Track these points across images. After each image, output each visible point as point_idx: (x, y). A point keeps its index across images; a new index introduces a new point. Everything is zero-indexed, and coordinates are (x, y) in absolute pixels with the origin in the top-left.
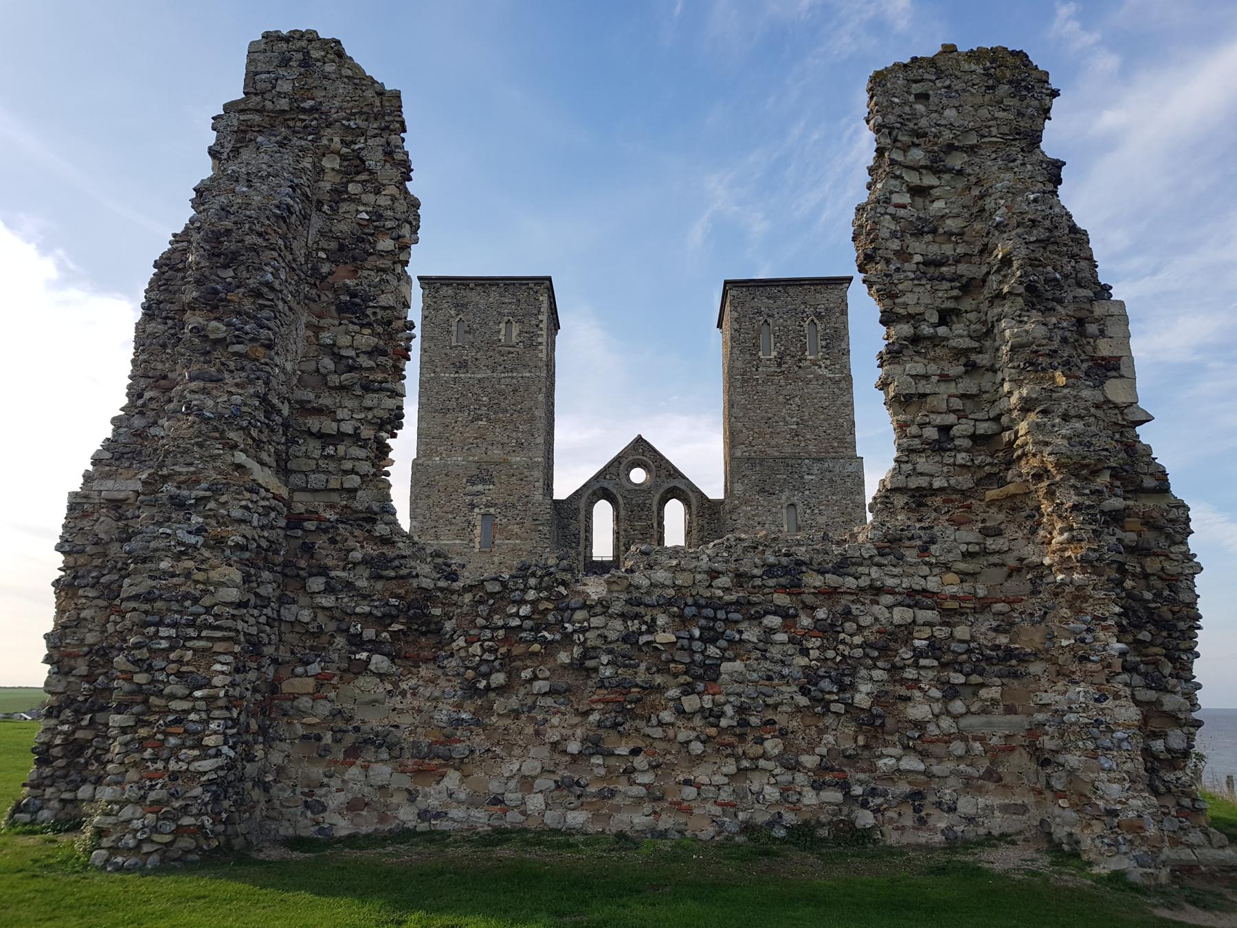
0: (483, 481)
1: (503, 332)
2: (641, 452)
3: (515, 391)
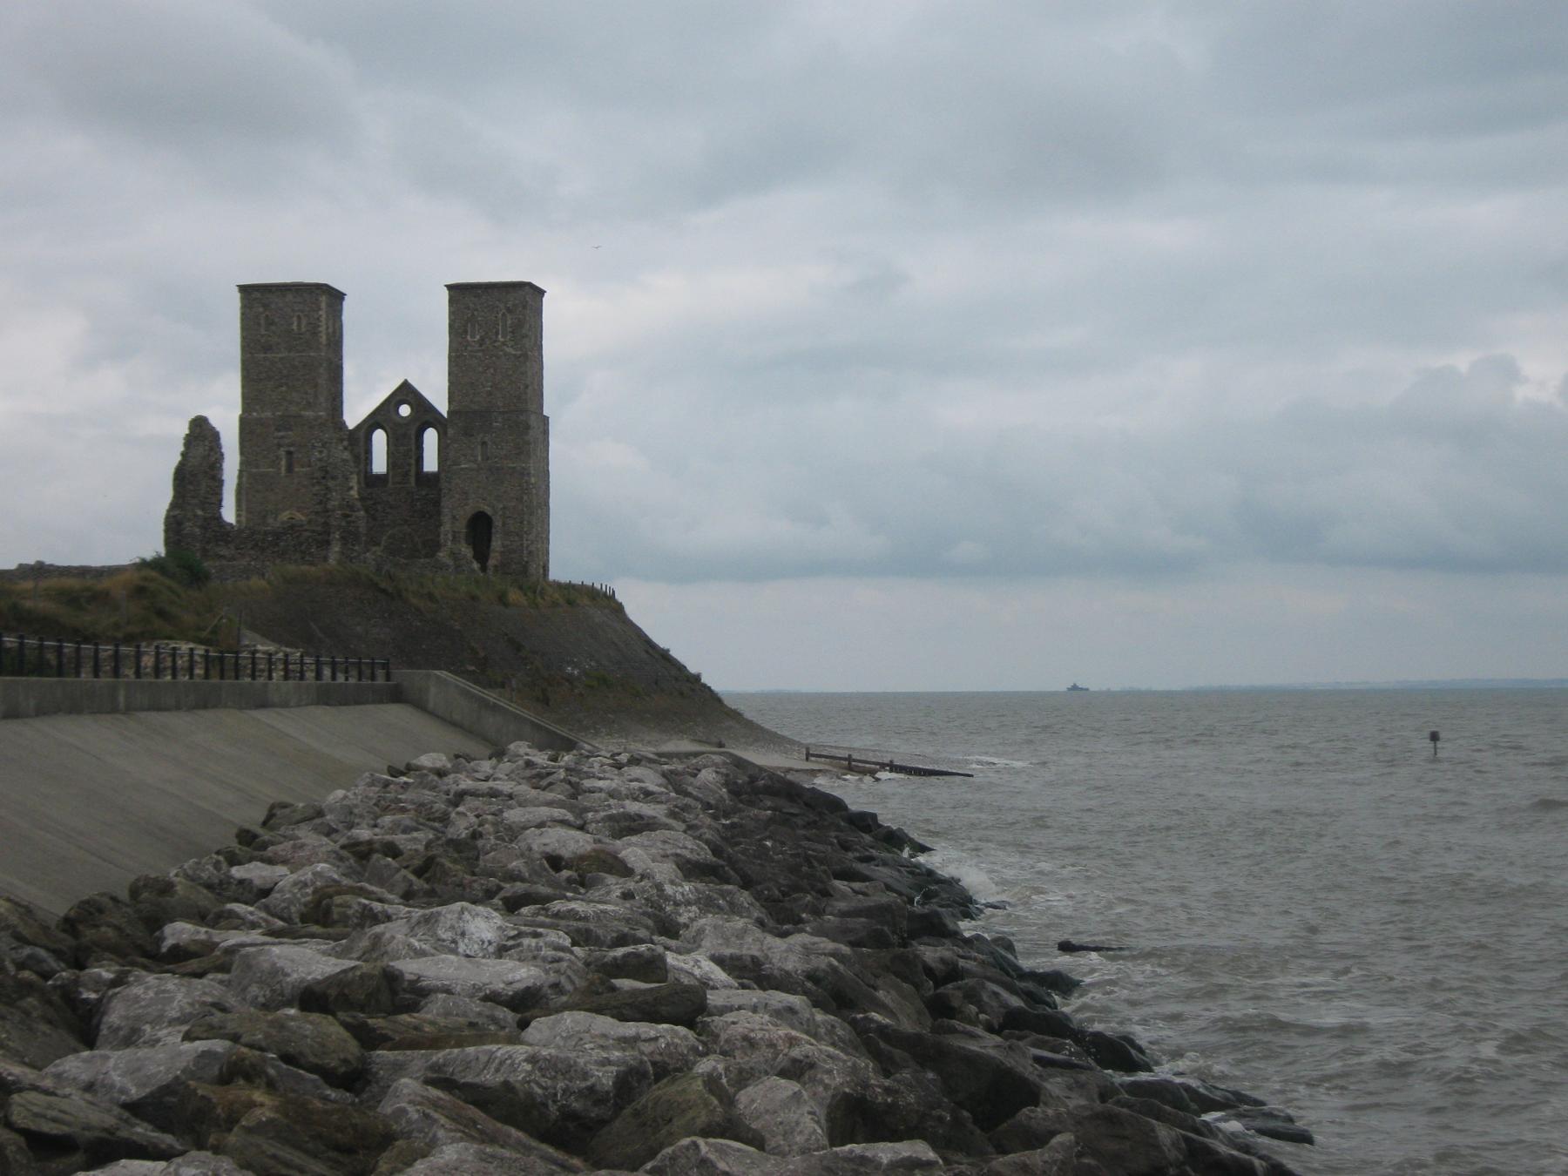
2: (406, 392)
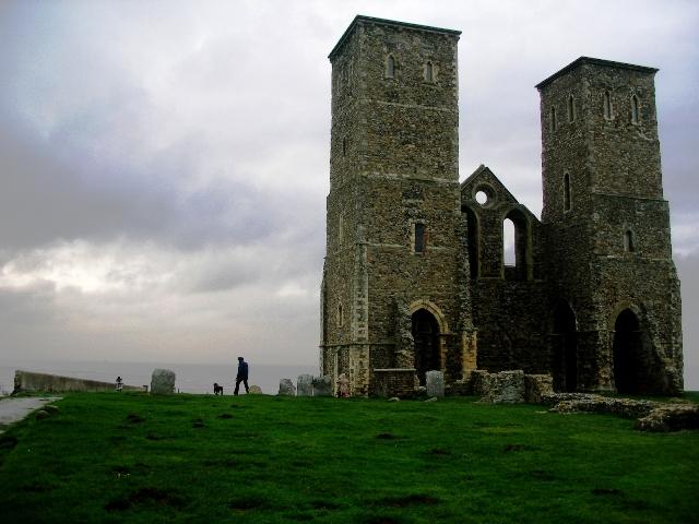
0: (416, 196)
1: (425, 72)
2: (484, 178)
3: (436, 122)
